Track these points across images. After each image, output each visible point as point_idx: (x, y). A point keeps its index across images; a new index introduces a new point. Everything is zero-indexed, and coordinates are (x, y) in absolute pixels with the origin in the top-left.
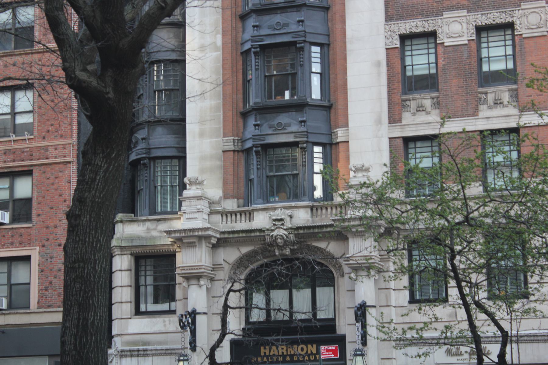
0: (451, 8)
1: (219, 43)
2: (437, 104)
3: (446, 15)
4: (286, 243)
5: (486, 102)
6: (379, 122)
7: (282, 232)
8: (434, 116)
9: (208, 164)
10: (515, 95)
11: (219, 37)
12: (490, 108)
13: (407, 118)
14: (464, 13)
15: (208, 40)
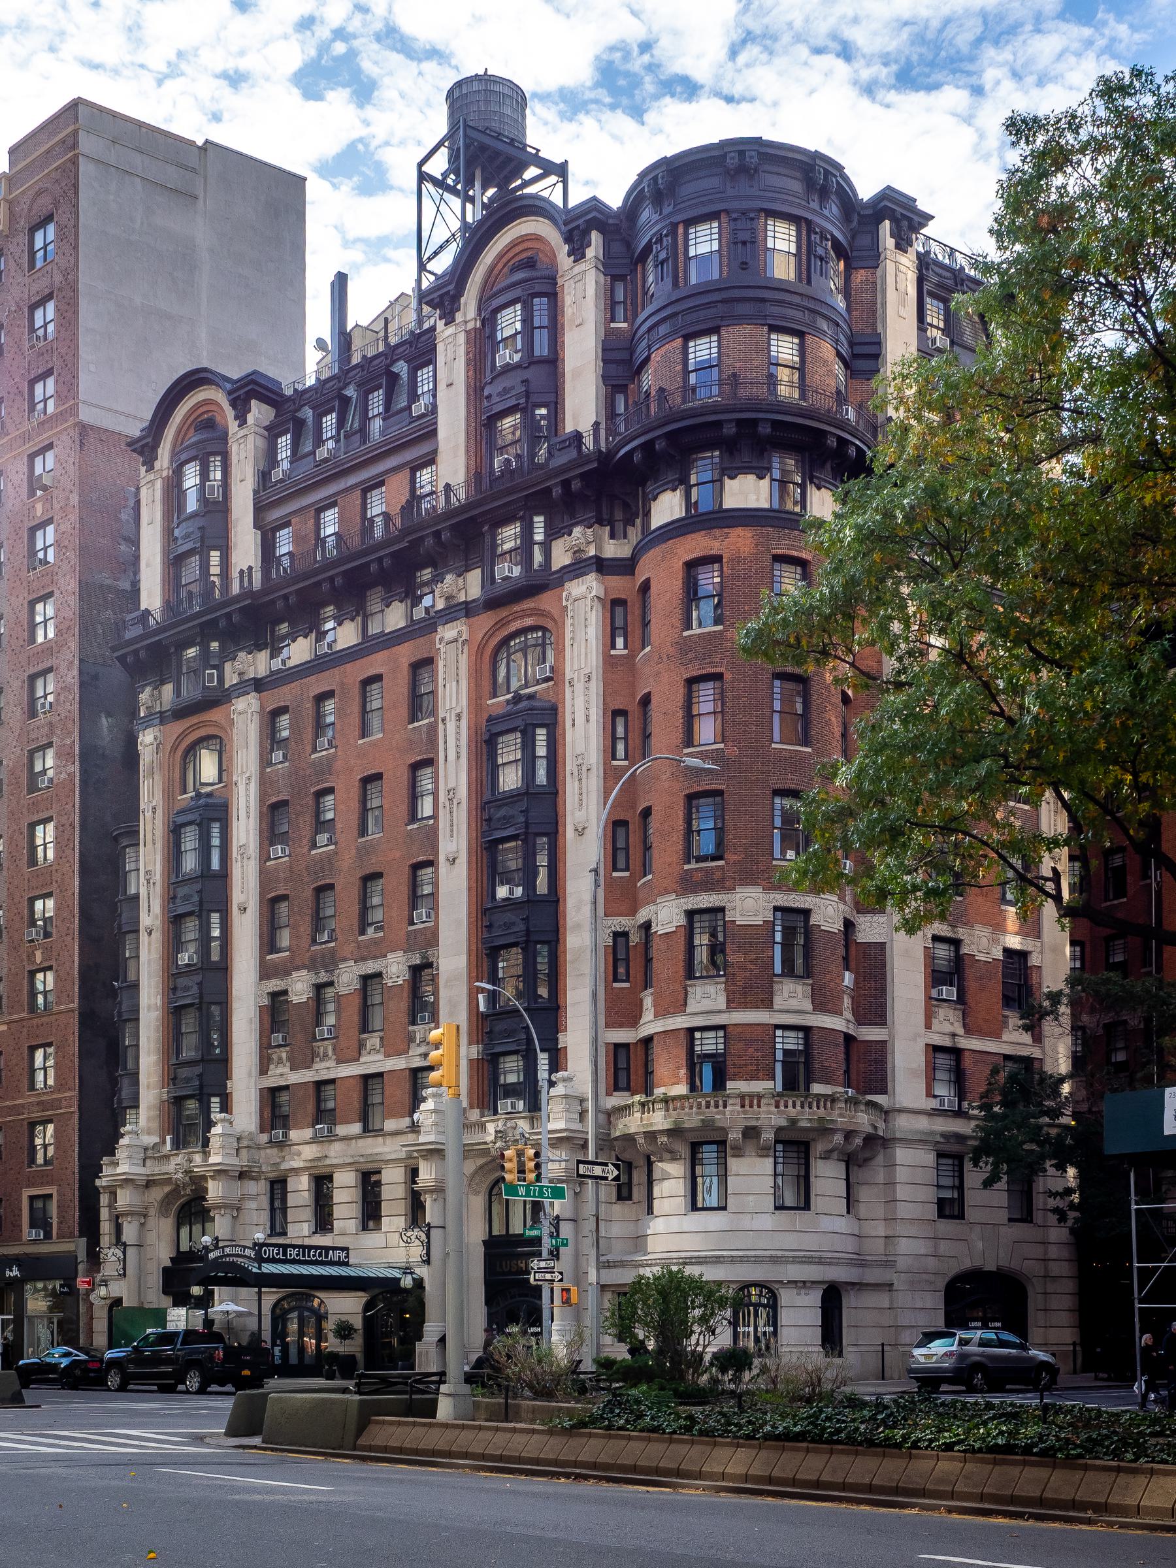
0: (299, 968)
1: (159, 1003)
2: (289, 1059)
3: (295, 974)
4: (185, 1186)
5: (318, 1055)
6: (250, 1075)
7: (180, 1175)
8: (286, 1070)
9: (152, 1113)
10: (334, 1049)
11: (159, 997)
12: (321, 1061)
13: (273, 1070)
14: (305, 972)
15: (153, 1001)
